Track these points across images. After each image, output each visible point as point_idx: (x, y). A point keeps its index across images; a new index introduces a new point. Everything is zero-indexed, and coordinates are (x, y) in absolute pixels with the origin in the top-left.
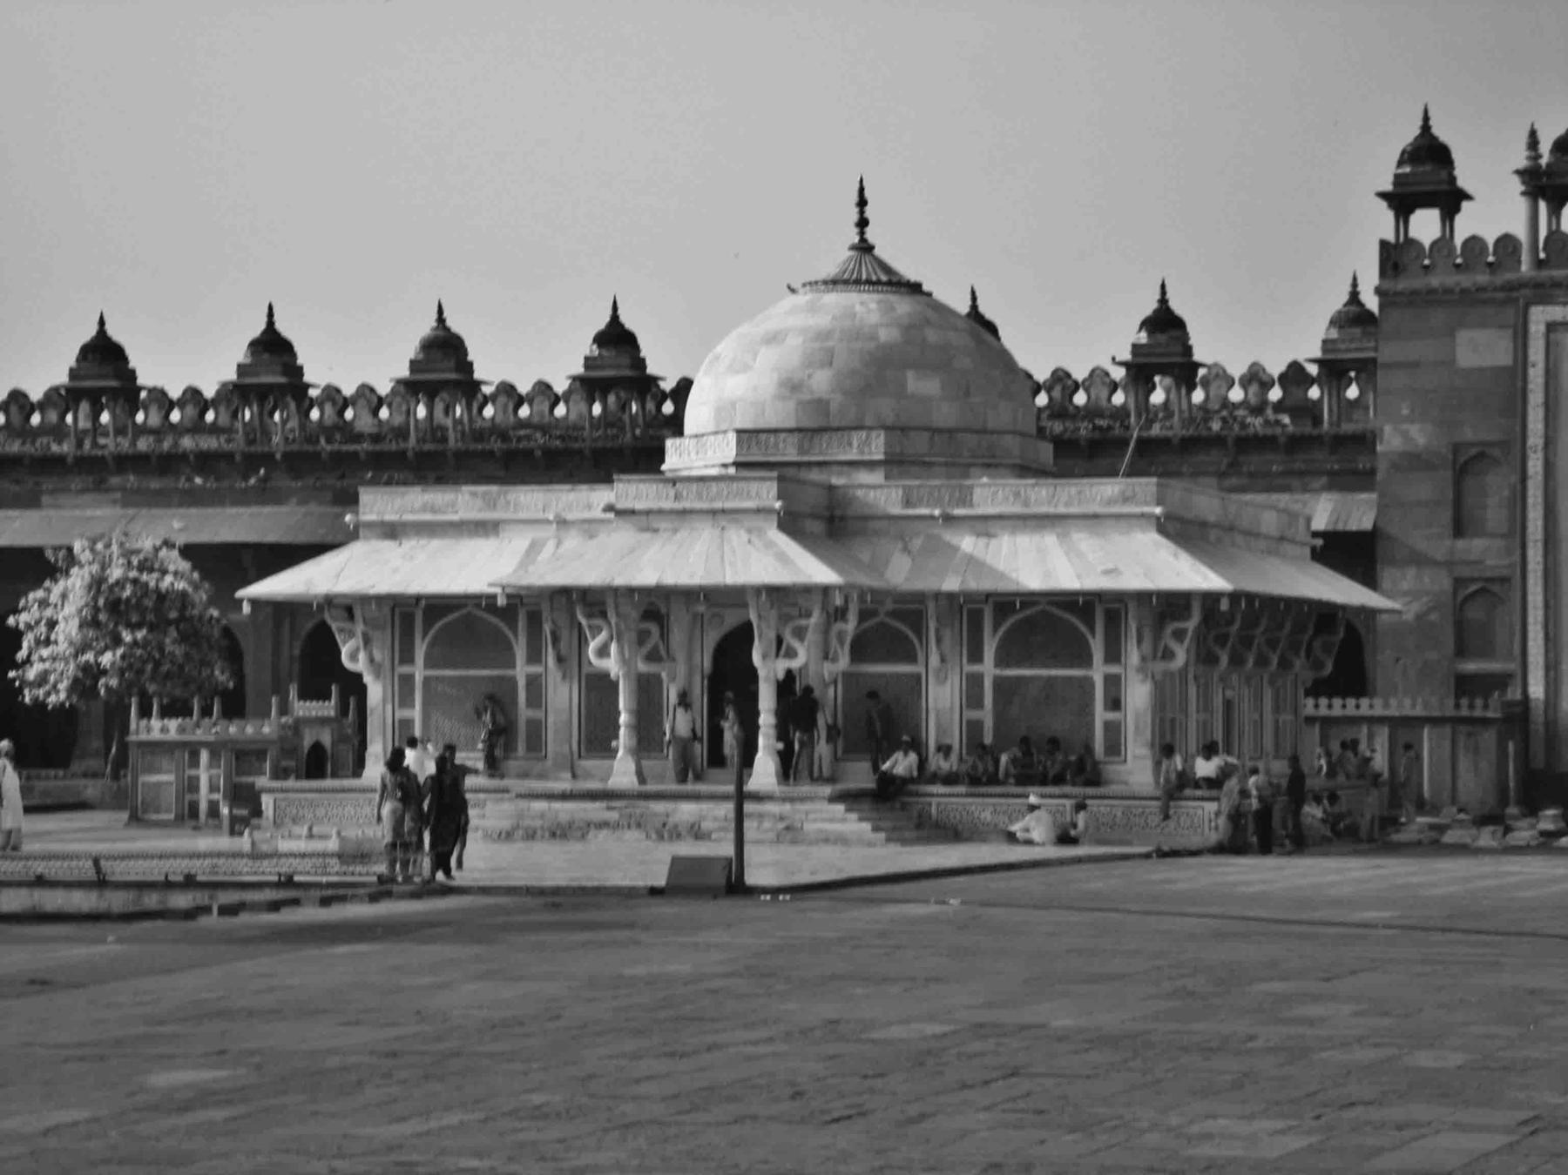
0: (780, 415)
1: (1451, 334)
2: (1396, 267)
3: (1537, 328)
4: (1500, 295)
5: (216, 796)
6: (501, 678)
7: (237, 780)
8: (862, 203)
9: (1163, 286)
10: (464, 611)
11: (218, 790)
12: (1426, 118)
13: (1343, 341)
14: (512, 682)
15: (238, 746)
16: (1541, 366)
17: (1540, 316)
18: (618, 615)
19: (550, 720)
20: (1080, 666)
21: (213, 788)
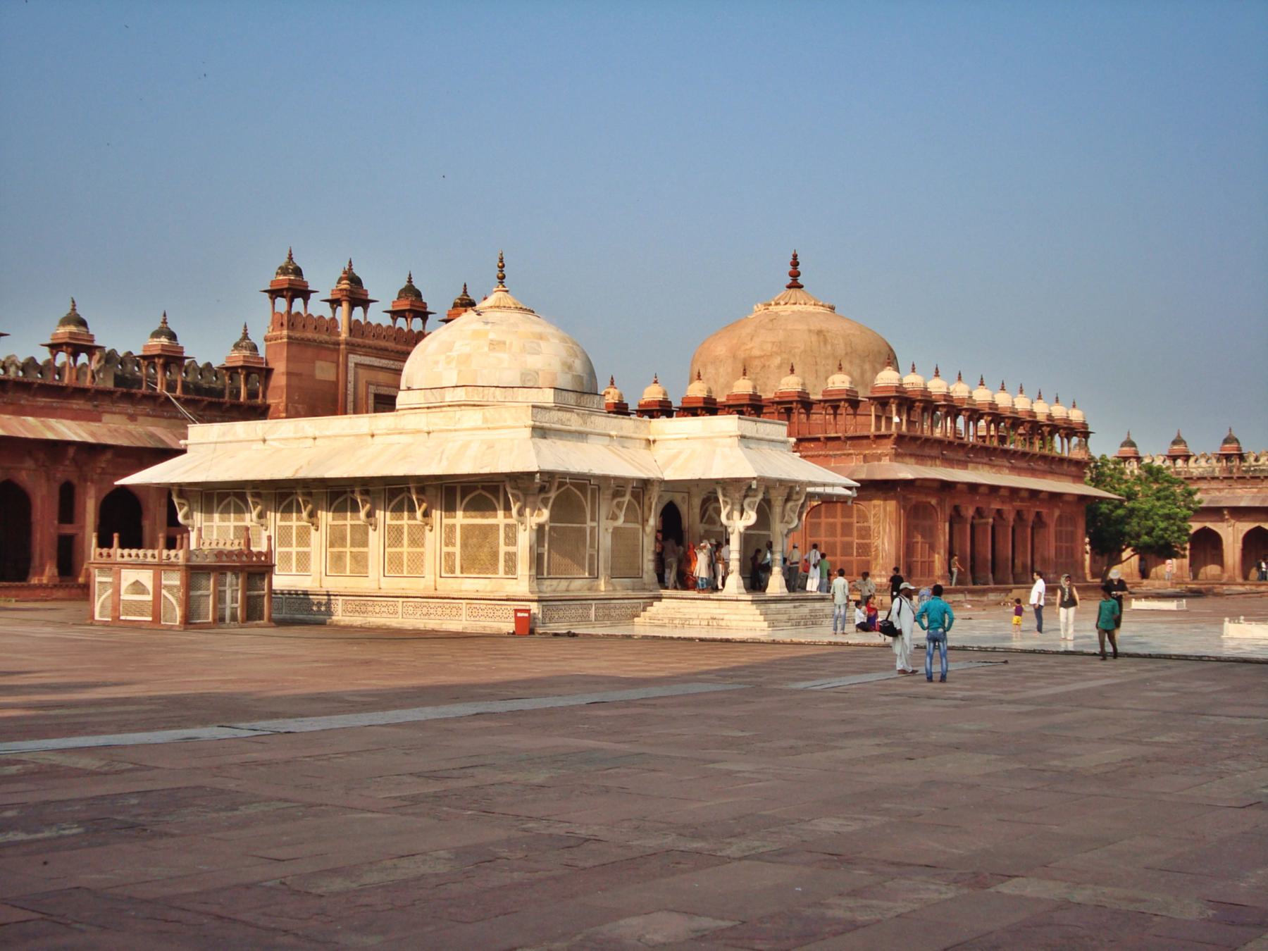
0: (565, 381)
1: (314, 363)
2: (293, 324)
3: (351, 365)
4: (331, 346)
5: (235, 605)
6: (581, 527)
7: (248, 593)
8: (503, 266)
9: (165, 315)
10: (566, 487)
11: (237, 602)
12: (290, 255)
13: (252, 357)
14: (584, 530)
15: (251, 569)
16: (352, 383)
17: (353, 359)
18: (724, 495)
19: (601, 553)
20: (764, 530)
21: (234, 600)
